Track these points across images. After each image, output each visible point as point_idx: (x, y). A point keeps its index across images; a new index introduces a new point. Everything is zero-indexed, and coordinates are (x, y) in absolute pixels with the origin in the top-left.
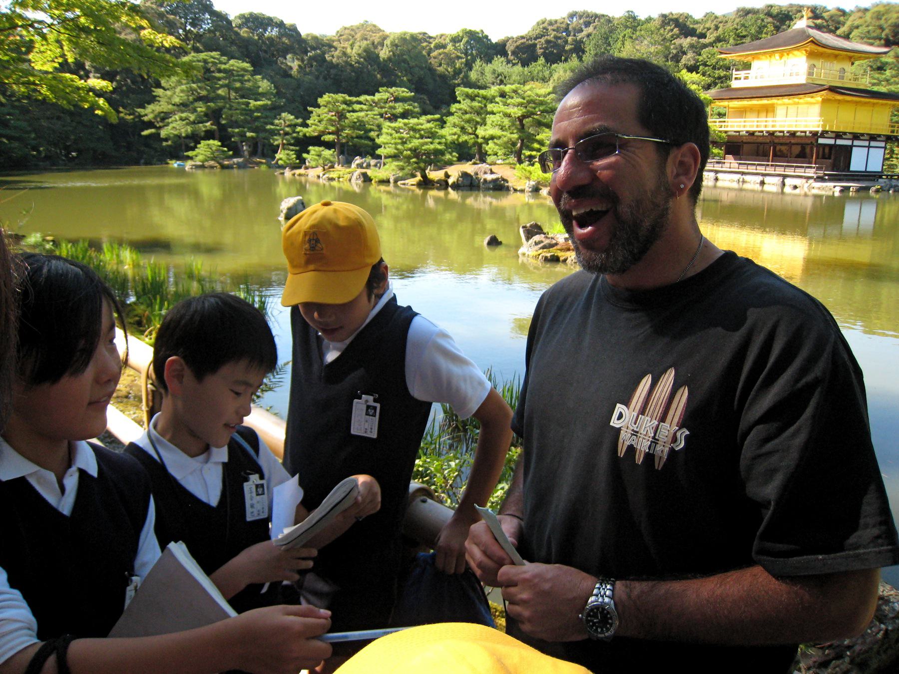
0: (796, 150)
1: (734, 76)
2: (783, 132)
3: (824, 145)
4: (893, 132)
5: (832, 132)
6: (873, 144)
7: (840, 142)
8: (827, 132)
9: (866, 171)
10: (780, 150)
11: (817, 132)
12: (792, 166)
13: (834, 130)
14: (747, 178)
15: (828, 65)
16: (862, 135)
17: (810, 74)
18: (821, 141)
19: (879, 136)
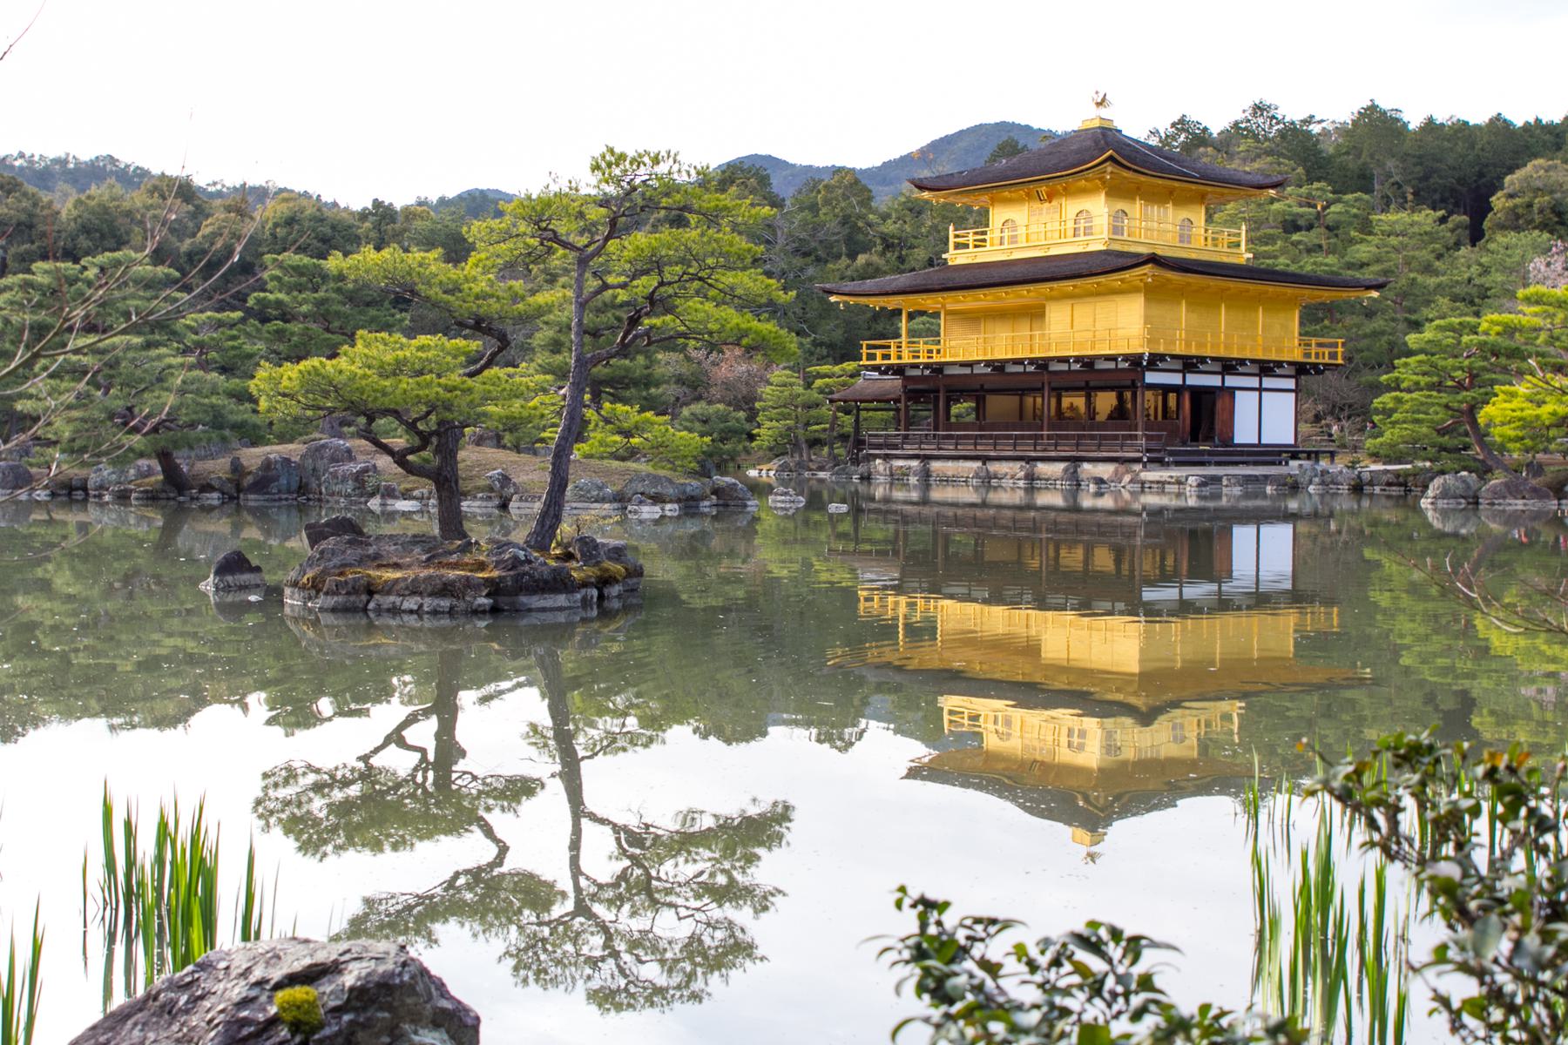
0: (1105, 402)
1: (952, 240)
2: (1064, 360)
3: (1166, 389)
4: (1308, 355)
5: (1173, 357)
6: (1268, 382)
7: (1194, 380)
8: (1162, 357)
9: (1260, 444)
10: (1072, 407)
11: (1141, 356)
12: (1092, 437)
13: (1177, 352)
14: (994, 467)
15: (1155, 210)
16: (1242, 362)
17: (1116, 230)
18: (1151, 377)
19: (1279, 364)
